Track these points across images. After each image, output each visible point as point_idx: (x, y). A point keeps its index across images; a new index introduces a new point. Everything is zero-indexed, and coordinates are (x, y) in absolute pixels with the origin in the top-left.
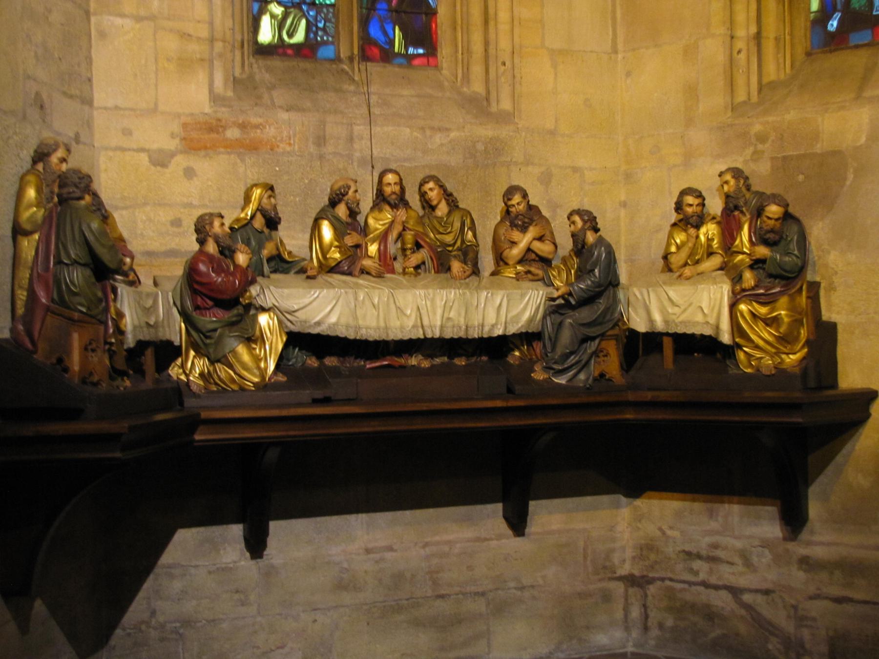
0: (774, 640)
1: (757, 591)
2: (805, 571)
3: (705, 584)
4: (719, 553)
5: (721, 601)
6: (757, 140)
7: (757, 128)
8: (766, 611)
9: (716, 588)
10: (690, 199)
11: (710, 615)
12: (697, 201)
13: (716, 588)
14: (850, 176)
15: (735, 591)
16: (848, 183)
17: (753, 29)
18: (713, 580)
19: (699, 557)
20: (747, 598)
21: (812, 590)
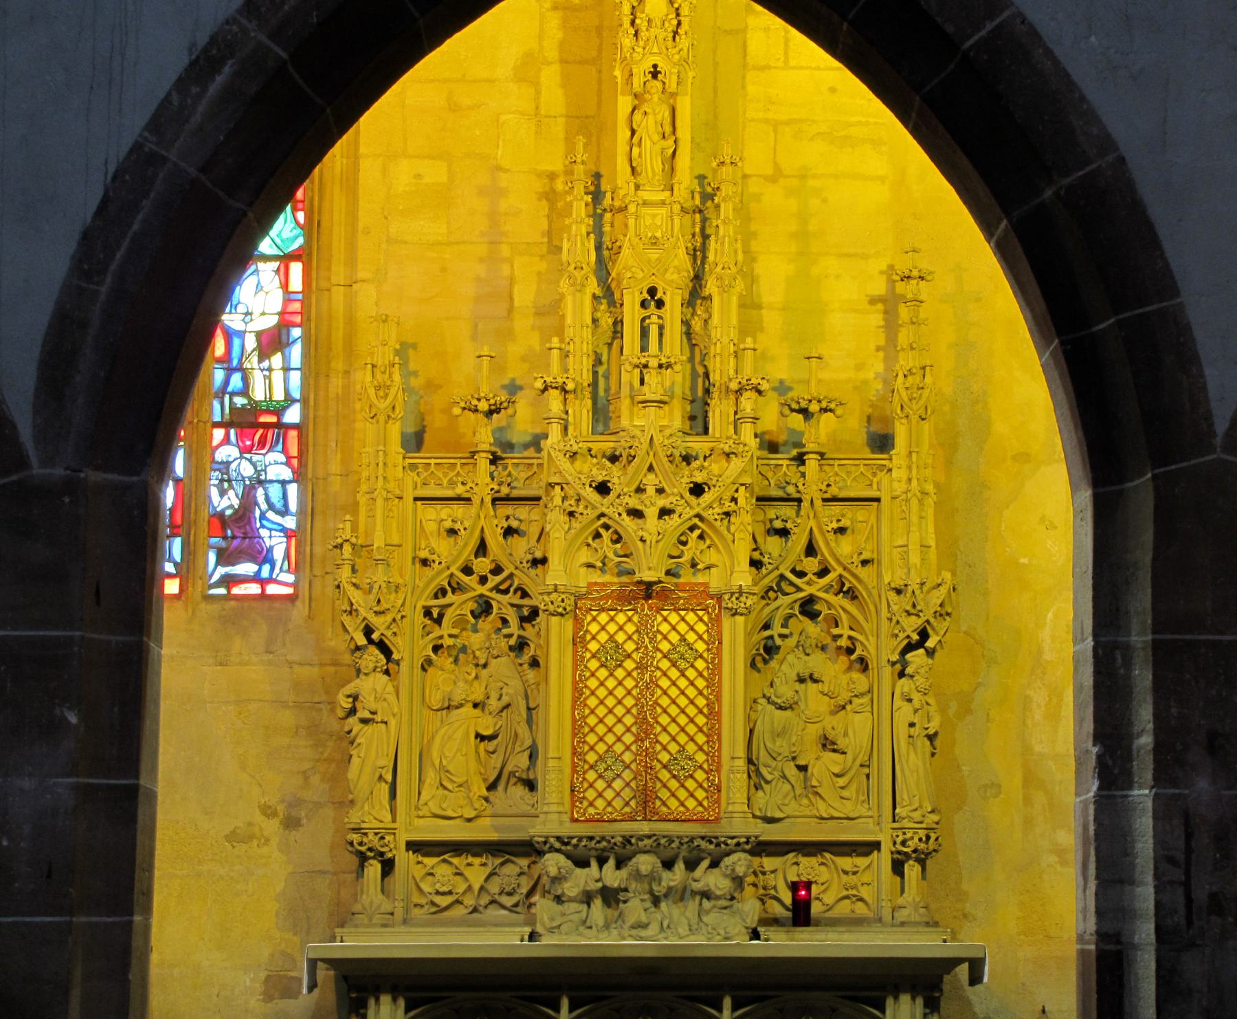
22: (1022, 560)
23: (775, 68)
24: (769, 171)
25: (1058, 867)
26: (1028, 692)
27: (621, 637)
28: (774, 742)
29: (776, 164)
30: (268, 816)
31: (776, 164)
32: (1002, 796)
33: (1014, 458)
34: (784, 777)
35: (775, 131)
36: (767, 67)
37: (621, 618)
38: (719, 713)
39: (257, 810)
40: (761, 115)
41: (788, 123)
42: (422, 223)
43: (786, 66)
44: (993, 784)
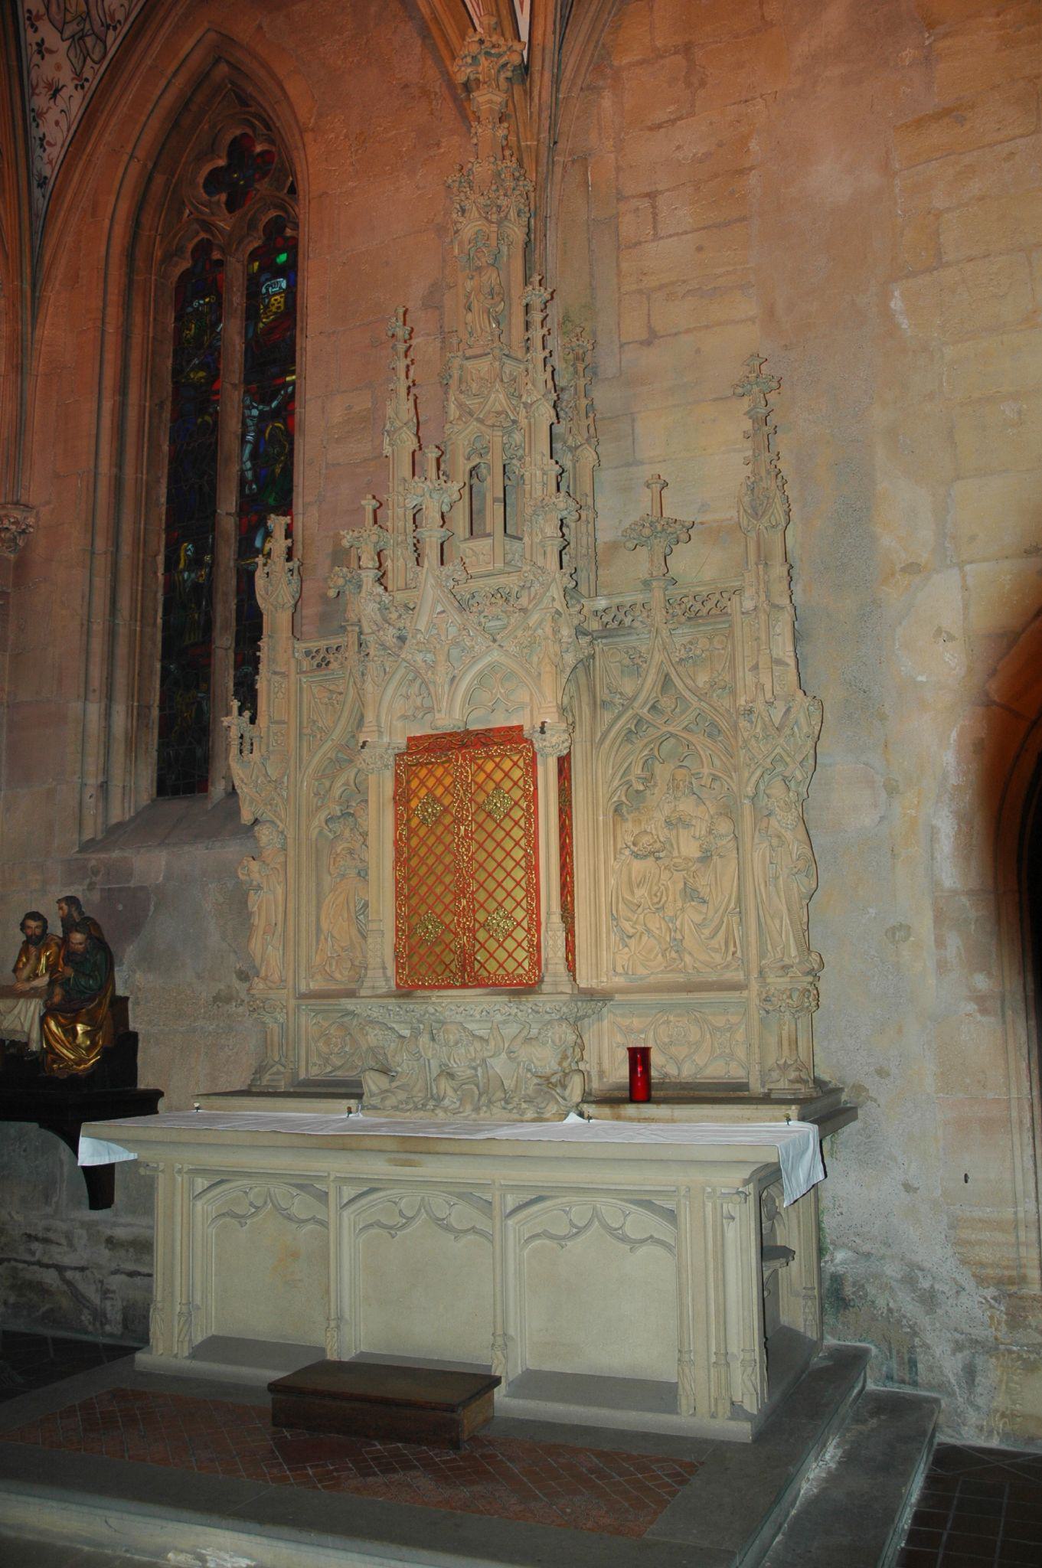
0: (86, 1311)
1: (76, 1268)
2: (110, 1250)
3: (40, 1264)
4: (51, 1235)
5: (50, 1277)
6: (93, 873)
7: (93, 863)
8: (82, 1287)
9: (48, 1266)
10: (32, 924)
11: (42, 1289)
12: (38, 923)
13: (48, 1266)
14: (152, 908)
15: (60, 1269)
16: (150, 913)
17: (101, 779)
18: (46, 1260)
19: (37, 1239)
20: (69, 1274)
21: (114, 1266)
22: (920, 678)
23: (646, 242)
24: (644, 336)
25: (979, 1017)
26: (934, 822)
27: (439, 792)
28: (633, 893)
29: (650, 327)
30: (241, 980)
31: (650, 327)
32: (912, 939)
33: (903, 570)
34: (648, 930)
35: (649, 298)
36: (640, 243)
37: (439, 772)
38: (536, 868)
39: (234, 975)
40: (634, 287)
41: (661, 287)
42: (351, 445)
43: (656, 237)
44: (901, 925)
